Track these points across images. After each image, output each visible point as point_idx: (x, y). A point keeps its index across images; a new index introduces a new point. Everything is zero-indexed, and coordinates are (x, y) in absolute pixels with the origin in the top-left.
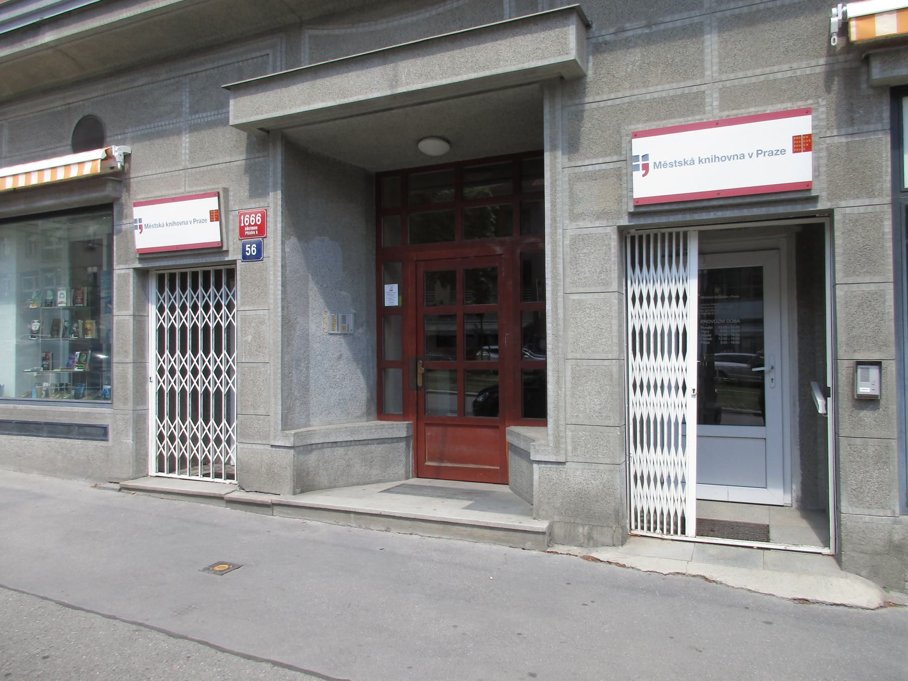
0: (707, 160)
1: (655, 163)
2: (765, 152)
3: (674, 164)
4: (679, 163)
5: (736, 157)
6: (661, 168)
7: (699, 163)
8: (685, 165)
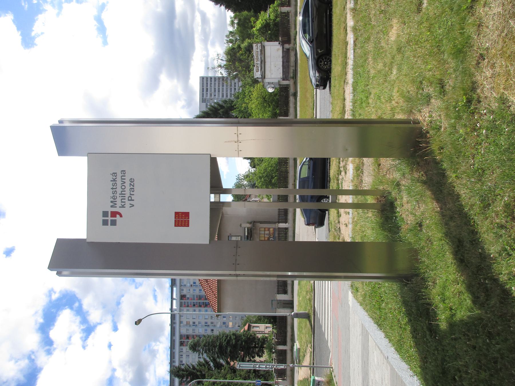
1: (112, 206)
3: (114, 190)
4: (114, 186)
6: (116, 201)
8: (116, 181)
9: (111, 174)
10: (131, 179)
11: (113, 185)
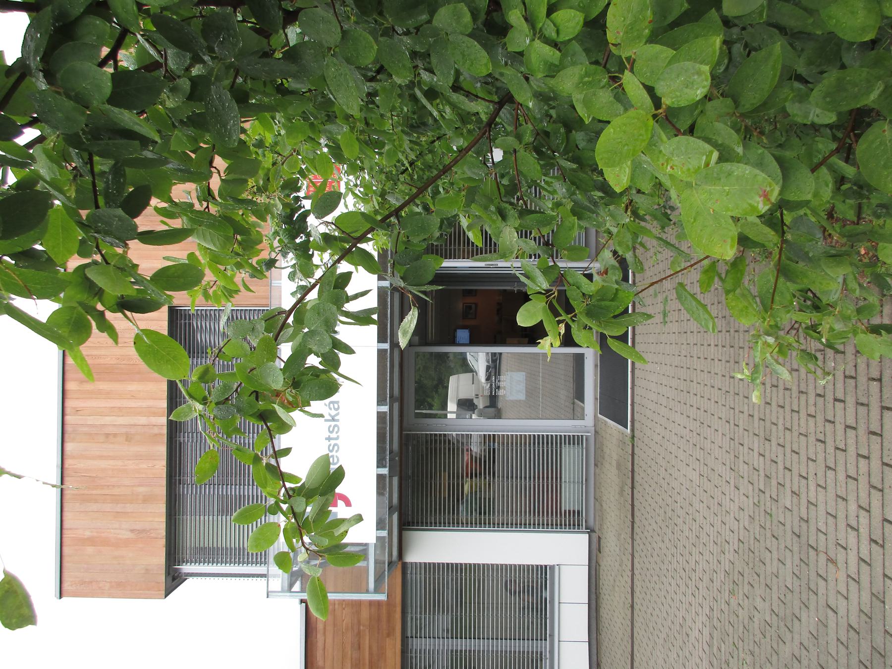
3: (333, 442)
4: (331, 432)
8: (338, 420)
11: (331, 429)
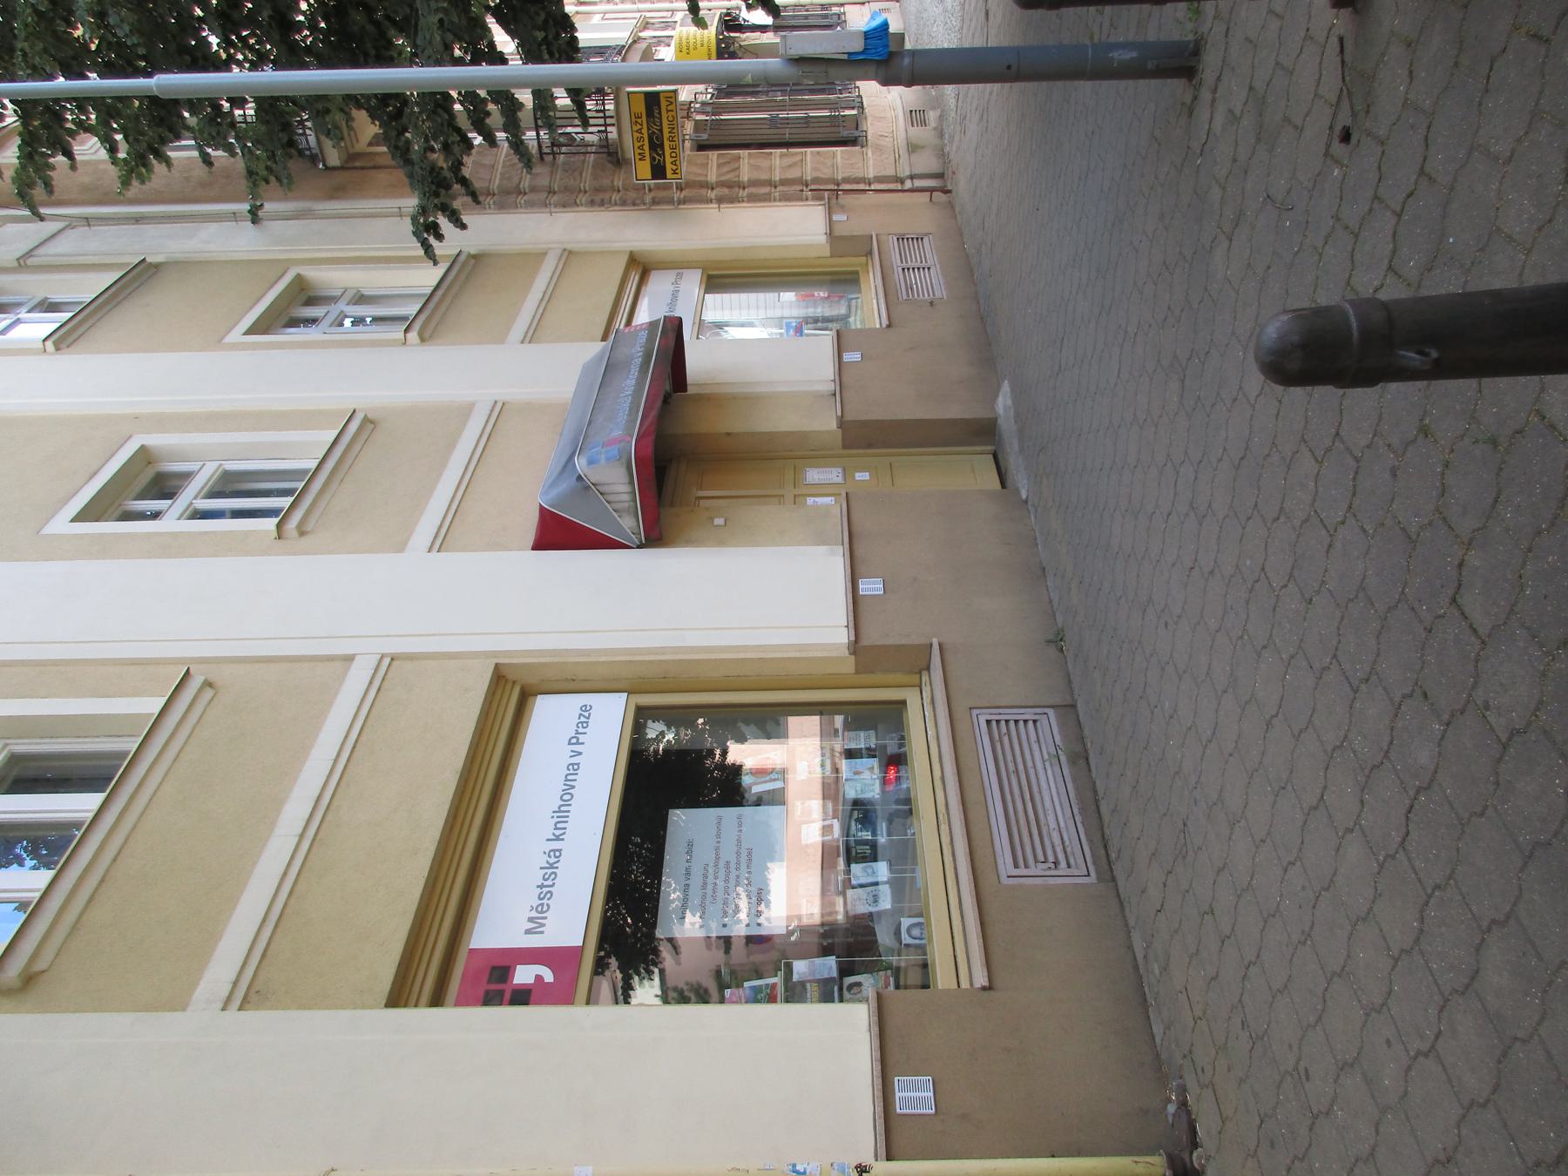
0: (559, 826)
2: (577, 733)
3: (545, 890)
4: (546, 880)
5: (569, 777)
6: (546, 918)
7: (563, 840)
8: (557, 868)
9: (545, 853)
10: (586, 706)
